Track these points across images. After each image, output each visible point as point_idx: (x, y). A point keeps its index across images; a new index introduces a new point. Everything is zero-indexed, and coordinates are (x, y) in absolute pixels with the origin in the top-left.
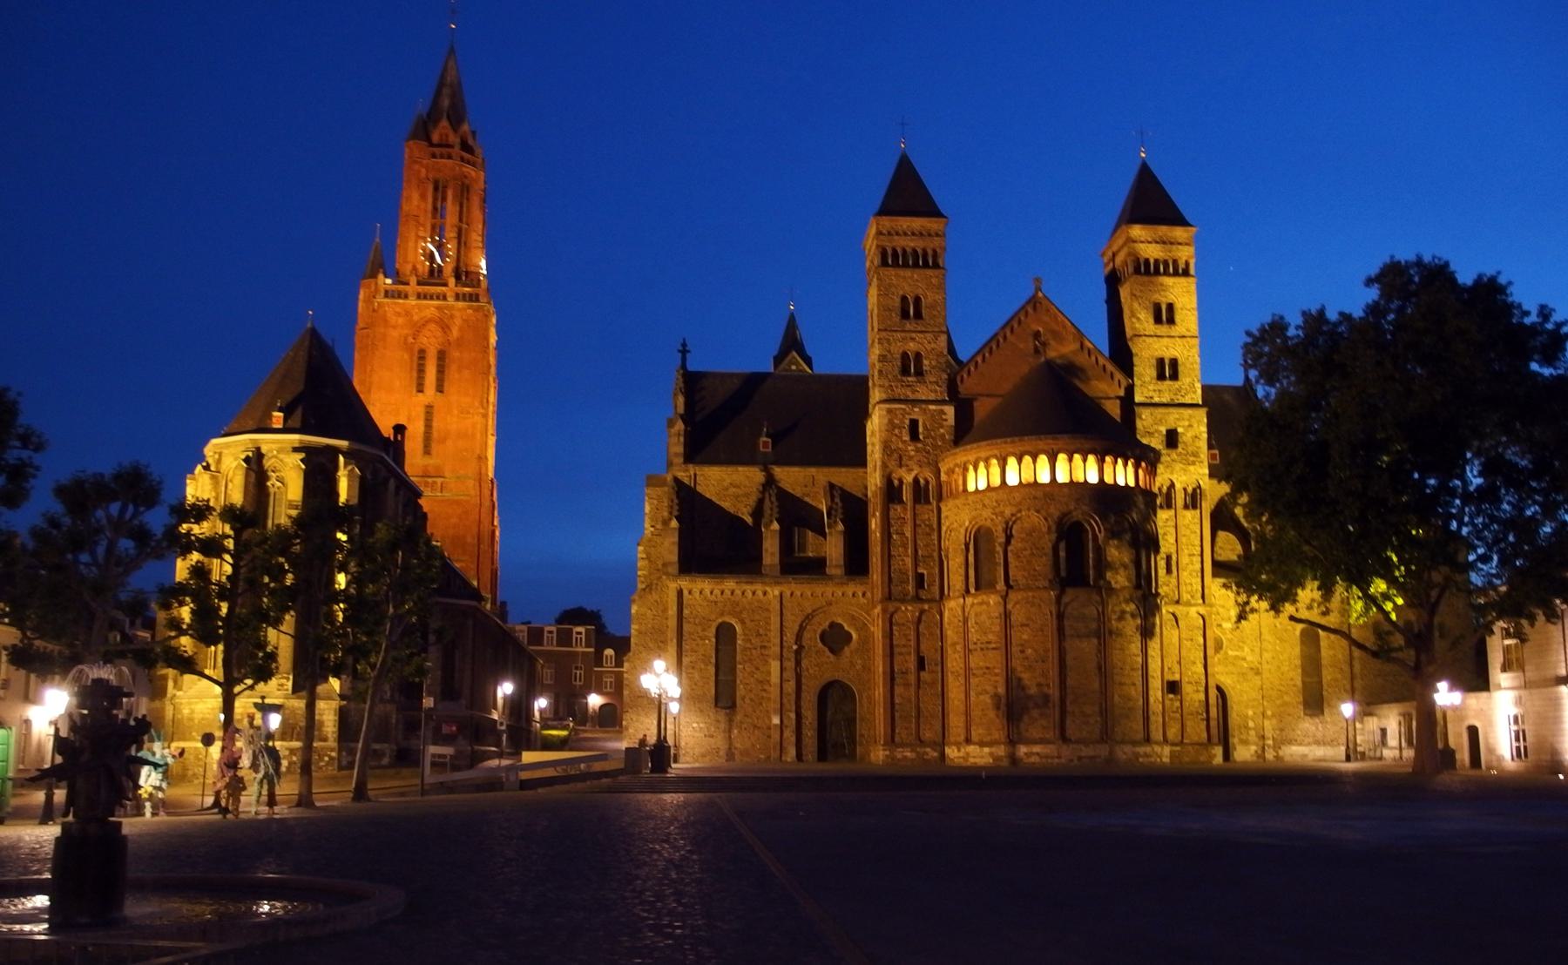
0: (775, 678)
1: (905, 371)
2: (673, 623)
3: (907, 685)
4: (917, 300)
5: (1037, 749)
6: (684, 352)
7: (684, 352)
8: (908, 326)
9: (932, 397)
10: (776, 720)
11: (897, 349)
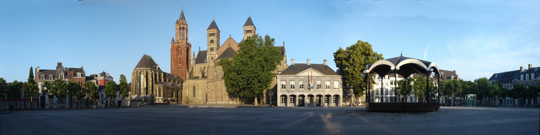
0: (200, 93)
1: (211, 50)
2: (188, 86)
3: (210, 93)
4: (213, 40)
5: (219, 102)
6: (200, 48)
7: (200, 48)
8: (211, 44)
9: (214, 54)
10: (200, 98)
11: (210, 47)
